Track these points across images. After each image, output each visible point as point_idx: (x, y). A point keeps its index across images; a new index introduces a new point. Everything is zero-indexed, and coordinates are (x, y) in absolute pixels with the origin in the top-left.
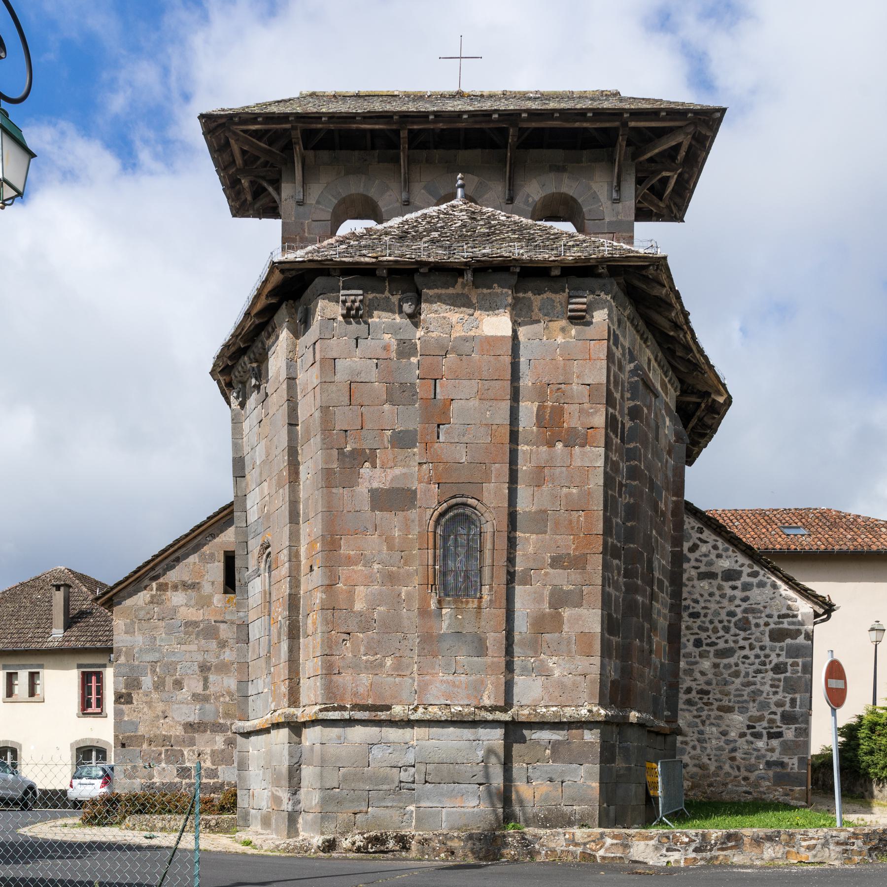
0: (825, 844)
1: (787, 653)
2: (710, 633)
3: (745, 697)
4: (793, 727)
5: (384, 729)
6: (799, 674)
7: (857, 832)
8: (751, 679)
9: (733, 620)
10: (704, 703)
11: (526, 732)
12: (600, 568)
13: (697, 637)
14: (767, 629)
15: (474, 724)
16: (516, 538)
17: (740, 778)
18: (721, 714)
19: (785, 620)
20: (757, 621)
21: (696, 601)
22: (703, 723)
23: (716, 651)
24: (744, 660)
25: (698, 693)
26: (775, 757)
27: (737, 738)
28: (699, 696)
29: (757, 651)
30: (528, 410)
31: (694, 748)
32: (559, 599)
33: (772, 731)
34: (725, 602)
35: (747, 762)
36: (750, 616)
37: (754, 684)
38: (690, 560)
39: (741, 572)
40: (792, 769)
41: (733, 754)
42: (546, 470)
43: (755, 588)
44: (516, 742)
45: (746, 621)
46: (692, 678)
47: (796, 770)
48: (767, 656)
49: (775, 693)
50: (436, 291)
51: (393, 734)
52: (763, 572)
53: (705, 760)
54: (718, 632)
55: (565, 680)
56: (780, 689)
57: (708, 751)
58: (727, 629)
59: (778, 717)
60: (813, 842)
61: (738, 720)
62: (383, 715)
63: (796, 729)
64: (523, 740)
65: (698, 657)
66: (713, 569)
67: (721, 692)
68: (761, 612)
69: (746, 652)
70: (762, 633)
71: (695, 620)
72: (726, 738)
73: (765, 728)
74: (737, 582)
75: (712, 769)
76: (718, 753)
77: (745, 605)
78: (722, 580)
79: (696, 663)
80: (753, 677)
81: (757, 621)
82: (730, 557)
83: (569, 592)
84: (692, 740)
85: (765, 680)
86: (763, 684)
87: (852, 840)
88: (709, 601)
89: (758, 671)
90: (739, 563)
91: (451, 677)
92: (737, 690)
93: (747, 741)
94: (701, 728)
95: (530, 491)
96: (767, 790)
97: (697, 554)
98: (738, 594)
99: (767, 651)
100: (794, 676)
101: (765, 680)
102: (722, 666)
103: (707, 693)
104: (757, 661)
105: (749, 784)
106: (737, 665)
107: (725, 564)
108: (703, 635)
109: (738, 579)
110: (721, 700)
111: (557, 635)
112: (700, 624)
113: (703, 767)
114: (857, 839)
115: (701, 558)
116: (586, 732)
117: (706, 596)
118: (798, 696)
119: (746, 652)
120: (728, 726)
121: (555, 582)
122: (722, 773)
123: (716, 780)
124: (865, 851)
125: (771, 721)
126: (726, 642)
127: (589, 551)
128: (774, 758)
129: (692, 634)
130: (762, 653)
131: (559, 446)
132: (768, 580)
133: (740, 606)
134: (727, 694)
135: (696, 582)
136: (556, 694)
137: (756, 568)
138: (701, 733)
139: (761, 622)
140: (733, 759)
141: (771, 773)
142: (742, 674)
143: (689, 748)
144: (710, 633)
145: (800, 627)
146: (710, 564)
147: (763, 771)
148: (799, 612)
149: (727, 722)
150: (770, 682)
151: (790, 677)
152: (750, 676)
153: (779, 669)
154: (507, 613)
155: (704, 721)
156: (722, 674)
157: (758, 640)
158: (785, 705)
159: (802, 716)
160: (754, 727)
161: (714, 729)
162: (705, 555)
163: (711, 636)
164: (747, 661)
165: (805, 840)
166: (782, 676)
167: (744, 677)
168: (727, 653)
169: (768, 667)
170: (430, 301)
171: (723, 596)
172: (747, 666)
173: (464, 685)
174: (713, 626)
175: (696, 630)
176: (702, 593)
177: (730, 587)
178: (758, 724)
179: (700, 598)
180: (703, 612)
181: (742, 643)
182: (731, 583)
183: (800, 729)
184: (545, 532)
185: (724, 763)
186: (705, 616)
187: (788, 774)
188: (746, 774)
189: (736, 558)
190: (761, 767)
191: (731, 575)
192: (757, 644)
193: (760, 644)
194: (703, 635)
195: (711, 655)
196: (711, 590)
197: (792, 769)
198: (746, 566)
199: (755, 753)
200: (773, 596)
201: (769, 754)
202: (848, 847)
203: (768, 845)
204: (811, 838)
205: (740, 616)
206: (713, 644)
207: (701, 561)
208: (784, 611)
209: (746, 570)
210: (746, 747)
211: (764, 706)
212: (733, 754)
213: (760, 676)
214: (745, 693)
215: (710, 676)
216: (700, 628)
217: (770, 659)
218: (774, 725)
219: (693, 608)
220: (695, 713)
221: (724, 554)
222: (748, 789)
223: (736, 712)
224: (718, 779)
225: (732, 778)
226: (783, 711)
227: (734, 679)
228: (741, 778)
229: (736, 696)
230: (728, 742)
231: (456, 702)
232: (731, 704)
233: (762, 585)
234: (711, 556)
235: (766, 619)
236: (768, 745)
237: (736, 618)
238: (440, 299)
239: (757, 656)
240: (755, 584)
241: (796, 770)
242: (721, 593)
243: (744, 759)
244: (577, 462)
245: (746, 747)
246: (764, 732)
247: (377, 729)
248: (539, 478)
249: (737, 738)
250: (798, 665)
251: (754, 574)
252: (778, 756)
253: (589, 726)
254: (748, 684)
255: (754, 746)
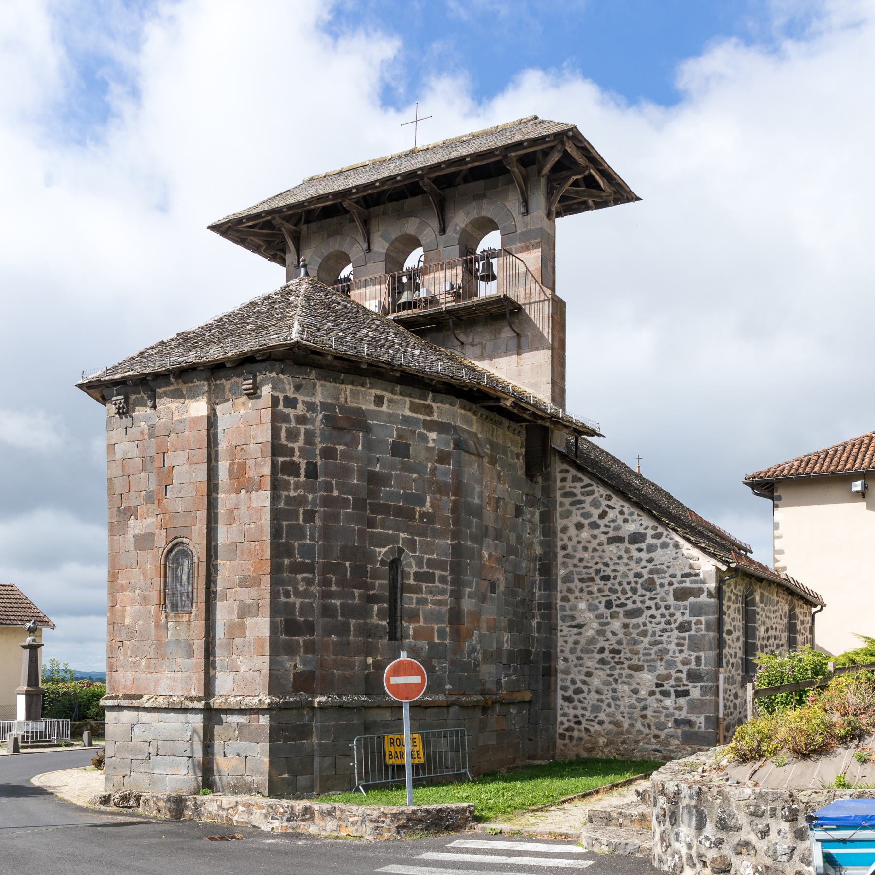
0: (363, 821)
1: (690, 612)
2: (619, 595)
3: (653, 656)
4: (699, 685)
5: (140, 713)
6: (703, 632)
7: (386, 812)
8: (657, 638)
9: (640, 581)
10: (615, 662)
11: (223, 716)
12: (269, 585)
13: (607, 598)
14: (671, 589)
15: (185, 710)
16: (217, 565)
17: (651, 736)
18: (632, 672)
19: (688, 579)
20: (662, 581)
21: (607, 565)
22: (616, 681)
23: (625, 611)
24: (651, 619)
25: (610, 652)
26: (683, 715)
27: (647, 696)
28: (611, 655)
29: (662, 610)
30: (223, 467)
31: (609, 705)
32: (245, 611)
33: (679, 689)
34: (633, 564)
35: (657, 720)
36: (655, 576)
37: (661, 642)
38: (600, 526)
39: (645, 534)
40: (699, 728)
41: (644, 712)
42: (235, 512)
43: (659, 550)
44: (217, 724)
45: (651, 581)
46: (605, 639)
47: (703, 729)
48: (672, 615)
49: (681, 651)
50: (163, 389)
51: (145, 716)
52: (667, 533)
53: (619, 718)
54: (627, 593)
55: (247, 674)
56: (685, 648)
57: (622, 709)
58: (634, 590)
59: (684, 676)
60: (356, 818)
61: (647, 679)
62: (136, 703)
63: (702, 688)
64: (220, 723)
65: (609, 618)
66: (621, 533)
67: (631, 652)
68: (665, 572)
69: (653, 612)
70: (667, 593)
71: (606, 583)
72: (638, 696)
73: (672, 687)
74: (643, 544)
75: (626, 726)
76: (631, 710)
77: (650, 566)
78: (629, 543)
79: (608, 624)
80: (660, 636)
81: (662, 581)
82: (635, 521)
83: (250, 606)
84: (607, 698)
85: (671, 639)
86: (669, 643)
87: (382, 819)
88: (618, 564)
89: (664, 631)
90: (644, 526)
91: (172, 674)
92: (645, 649)
93: (656, 700)
94: (614, 686)
95: (225, 527)
96: (676, 748)
97: (606, 521)
98: (644, 555)
99: (672, 610)
100: (698, 634)
101: (671, 639)
102: (631, 626)
103: (618, 652)
104: (663, 620)
105: (659, 742)
106: (645, 624)
107: (631, 528)
108: (613, 597)
109: (643, 541)
110: (631, 659)
111: (242, 639)
112: (611, 586)
113: (617, 724)
114: (386, 818)
115: (609, 524)
116: (261, 716)
117: (616, 560)
118: (702, 654)
119: (653, 612)
120: (638, 684)
121: (241, 598)
122: (634, 730)
123: (628, 738)
124: (393, 829)
125: (678, 679)
126: (634, 602)
127: (261, 573)
128: (682, 717)
129: (603, 596)
130: (667, 612)
131: (243, 492)
132: (671, 541)
133: (645, 567)
134: (637, 653)
135: (606, 547)
136: (242, 686)
137: (660, 529)
138: (614, 691)
139: (666, 582)
140: (644, 717)
141: (679, 732)
142: (650, 634)
143: (604, 706)
144: (619, 595)
145: (702, 585)
146: (617, 528)
147: (672, 730)
148: (701, 571)
149: (638, 680)
150: (676, 641)
151: (694, 636)
152: (657, 635)
153: (683, 627)
154: (206, 626)
155: (617, 680)
156: (631, 634)
157: (663, 599)
158: (690, 664)
159: (707, 674)
160: (662, 686)
161: (626, 687)
162: (614, 521)
163: (621, 597)
164: (654, 621)
165: (351, 817)
166: (686, 635)
167: (652, 636)
168: (635, 613)
169: (673, 626)
170: (160, 397)
171: (630, 558)
172: (654, 625)
173: (180, 680)
174: (621, 587)
175: (607, 593)
176: (612, 556)
177: (637, 550)
178: (666, 682)
179: (609, 562)
180: (612, 575)
181: (648, 603)
182: (637, 546)
183: (706, 687)
184: (235, 560)
185: (636, 720)
186: (615, 578)
187: (696, 733)
188: (656, 732)
189: (641, 522)
190: (670, 726)
191: (637, 538)
192: (662, 604)
193: (665, 603)
194: (613, 597)
195: (621, 615)
196: (620, 553)
197: (699, 728)
198: (650, 528)
199: (665, 711)
200: (676, 556)
201: (677, 712)
202: (379, 825)
203: (328, 818)
204: (355, 815)
205: (646, 577)
206: (622, 605)
207: (609, 527)
208: (687, 570)
209: (650, 532)
210: (655, 705)
211: (671, 664)
212: (644, 712)
213: (666, 634)
214: (652, 652)
215: (621, 636)
216: (610, 590)
217: (675, 618)
218: (681, 684)
219: (604, 571)
220: (608, 672)
221: (630, 518)
222: (657, 747)
223: (645, 670)
224: (630, 736)
225: (643, 736)
226: (689, 670)
227: (642, 638)
228: (652, 735)
229: (644, 655)
230: (639, 700)
231: (175, 694)
232: (640, 663)
233: (665, 546)
234: (618, 521)
235: (670, 579)
236: (676, 703)
237: (643, 579)
238: (166, 394)
239: (663, 616)
240: (658, 545)
241: (703, 729)
242: (628, 556)
243: (654, 717)
244: (254, 504)
245: (655, 705)
246: (672, 690)
247: (135, 713)
248: (232, 519)
249: (647, 696)
250: (701, 624)
251: (658, 536)
252: (686, 715)
253: (263, 712)
254: (655, 643)
255: (662, 704)
